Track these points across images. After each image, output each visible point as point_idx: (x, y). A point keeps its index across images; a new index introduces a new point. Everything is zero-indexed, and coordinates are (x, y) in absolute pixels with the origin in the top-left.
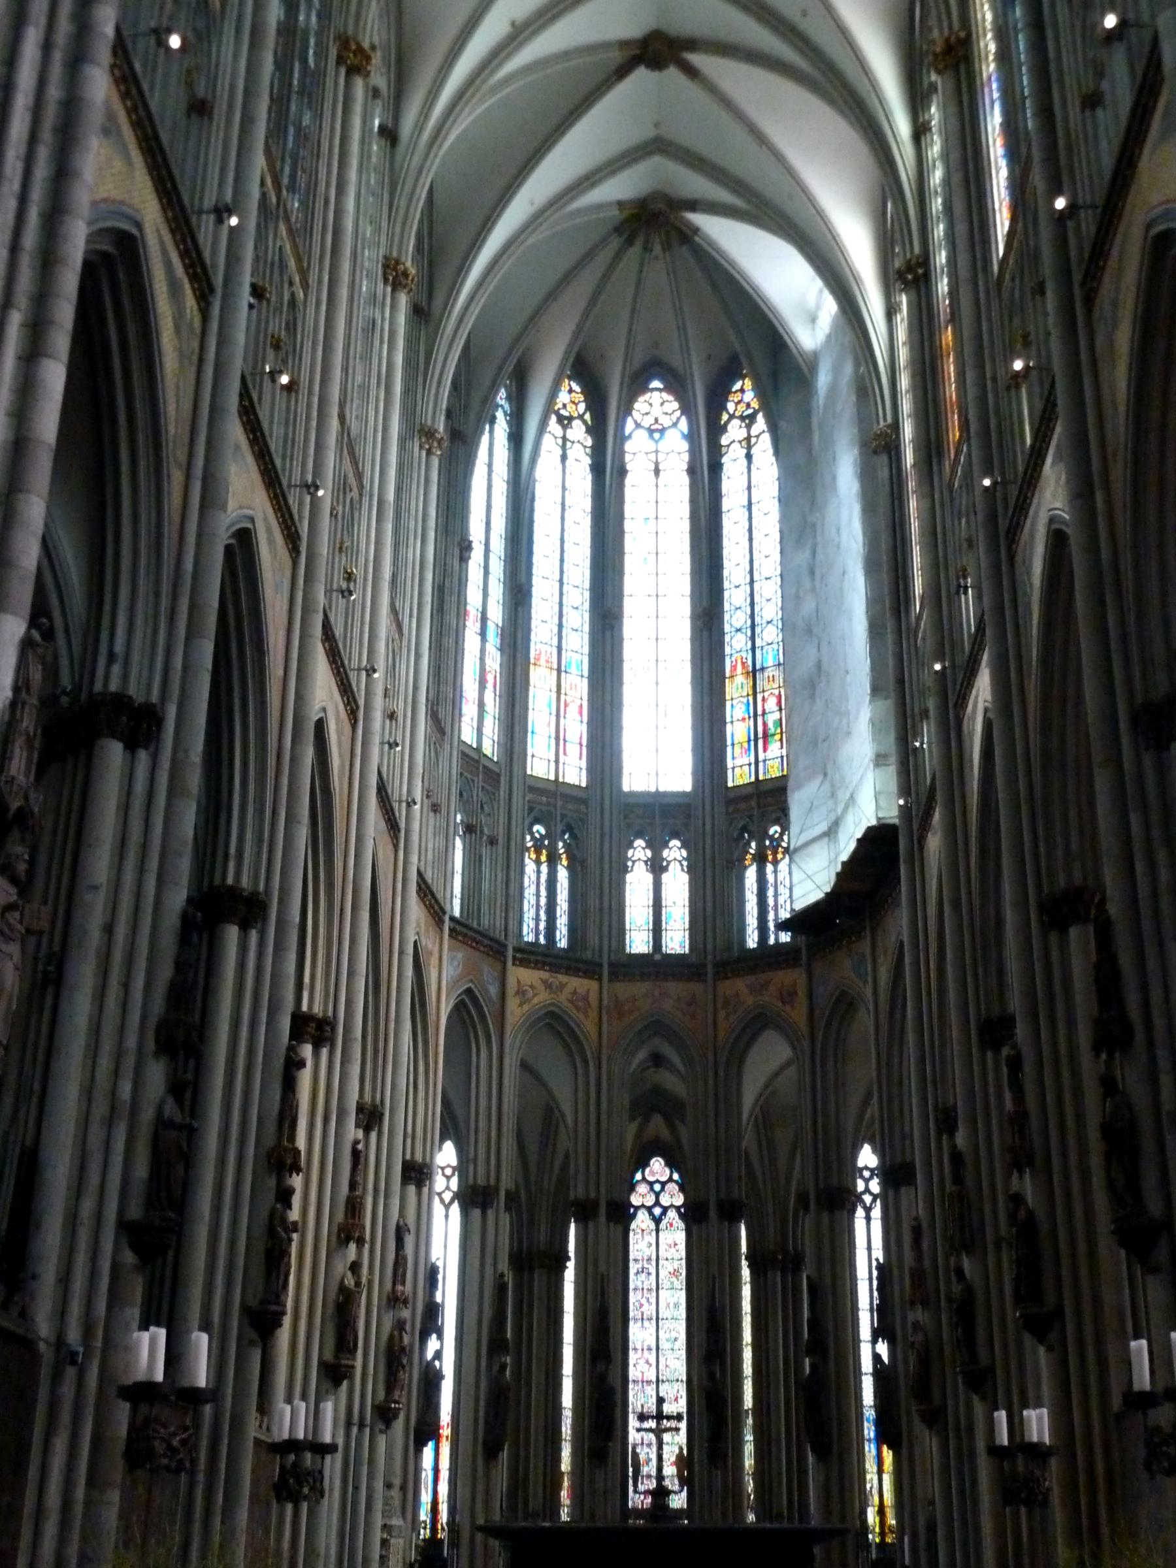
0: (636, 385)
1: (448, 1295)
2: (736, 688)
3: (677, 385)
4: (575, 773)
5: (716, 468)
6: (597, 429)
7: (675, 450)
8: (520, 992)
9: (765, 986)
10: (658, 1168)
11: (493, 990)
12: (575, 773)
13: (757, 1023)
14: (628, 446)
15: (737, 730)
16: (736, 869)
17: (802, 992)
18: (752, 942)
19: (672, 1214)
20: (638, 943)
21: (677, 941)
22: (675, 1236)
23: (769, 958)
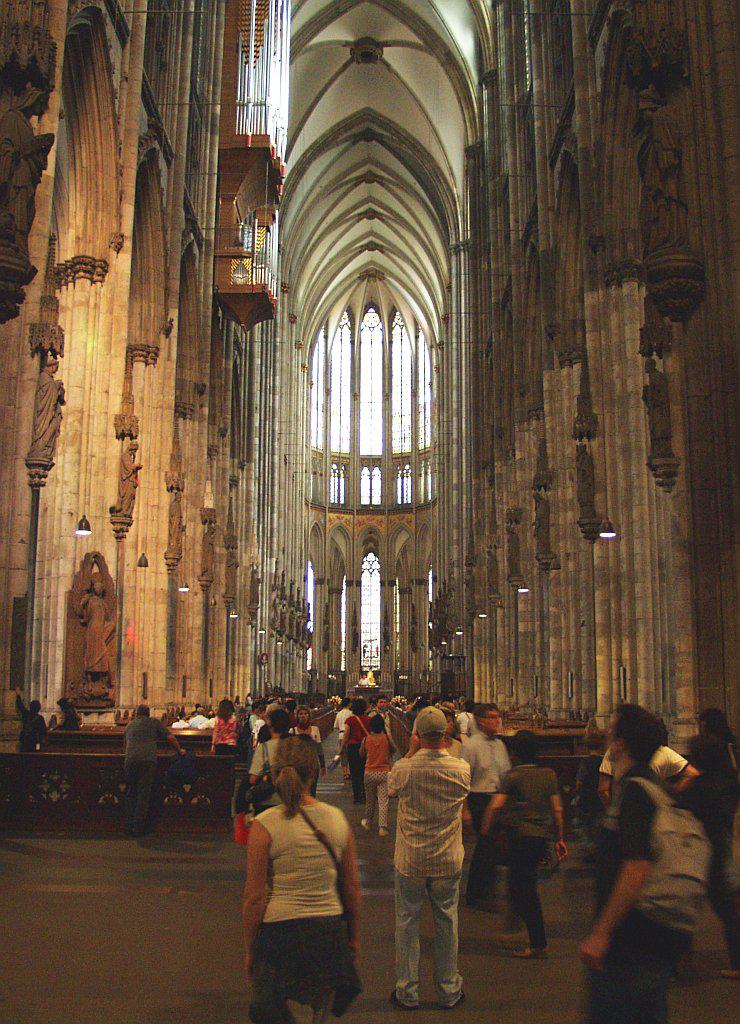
0: (366, 312)
1: (311, 611)
2: (396, 421)
3: (378, 311)
4: (346, 449)
5: (391, 342)
6: (352, 328)
7: (378, 335)
8: (330, 520)
9: (403, 518)
10: (371, 556)
11: (322, 521)
12: (346, 449)
13: (402, 529)
14: (363, 333)
15: (396, 436)
16: (394, 479)
17: (413, 521)
18: (399, 502)
19: (376, 571)
20: (365, 501)
21: (377, 501)
22: (377, 577)
23: (405, 508)
